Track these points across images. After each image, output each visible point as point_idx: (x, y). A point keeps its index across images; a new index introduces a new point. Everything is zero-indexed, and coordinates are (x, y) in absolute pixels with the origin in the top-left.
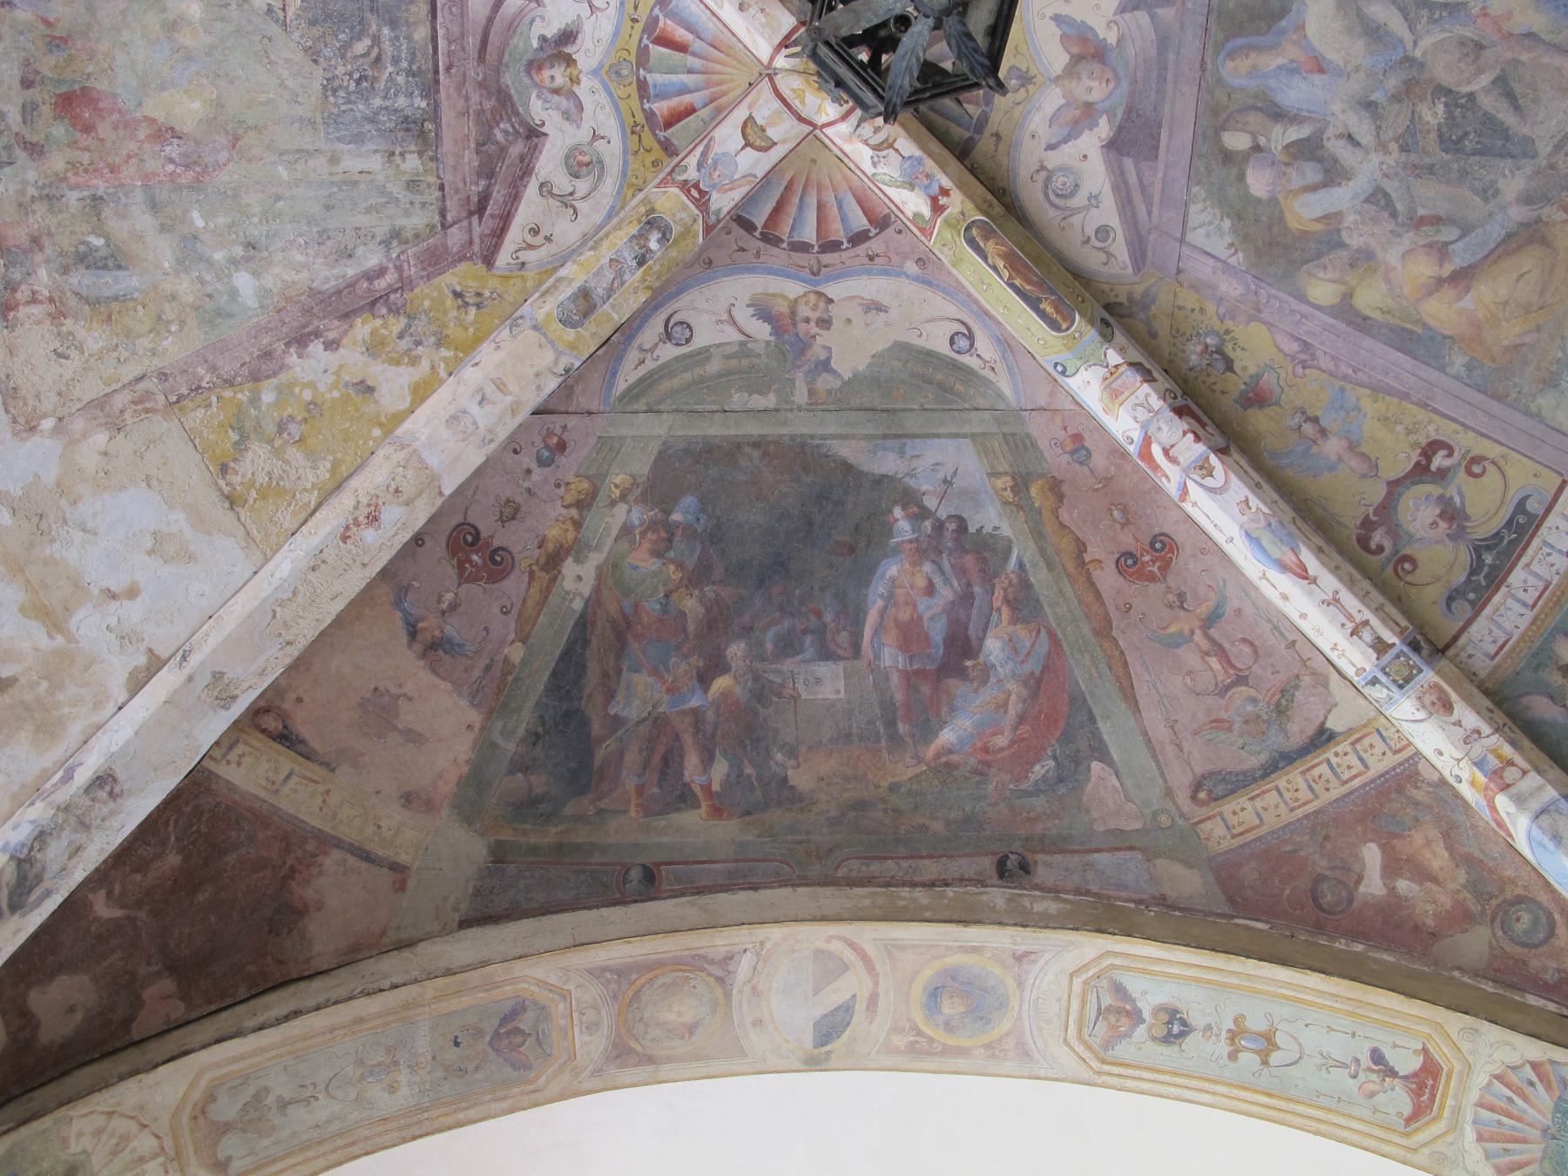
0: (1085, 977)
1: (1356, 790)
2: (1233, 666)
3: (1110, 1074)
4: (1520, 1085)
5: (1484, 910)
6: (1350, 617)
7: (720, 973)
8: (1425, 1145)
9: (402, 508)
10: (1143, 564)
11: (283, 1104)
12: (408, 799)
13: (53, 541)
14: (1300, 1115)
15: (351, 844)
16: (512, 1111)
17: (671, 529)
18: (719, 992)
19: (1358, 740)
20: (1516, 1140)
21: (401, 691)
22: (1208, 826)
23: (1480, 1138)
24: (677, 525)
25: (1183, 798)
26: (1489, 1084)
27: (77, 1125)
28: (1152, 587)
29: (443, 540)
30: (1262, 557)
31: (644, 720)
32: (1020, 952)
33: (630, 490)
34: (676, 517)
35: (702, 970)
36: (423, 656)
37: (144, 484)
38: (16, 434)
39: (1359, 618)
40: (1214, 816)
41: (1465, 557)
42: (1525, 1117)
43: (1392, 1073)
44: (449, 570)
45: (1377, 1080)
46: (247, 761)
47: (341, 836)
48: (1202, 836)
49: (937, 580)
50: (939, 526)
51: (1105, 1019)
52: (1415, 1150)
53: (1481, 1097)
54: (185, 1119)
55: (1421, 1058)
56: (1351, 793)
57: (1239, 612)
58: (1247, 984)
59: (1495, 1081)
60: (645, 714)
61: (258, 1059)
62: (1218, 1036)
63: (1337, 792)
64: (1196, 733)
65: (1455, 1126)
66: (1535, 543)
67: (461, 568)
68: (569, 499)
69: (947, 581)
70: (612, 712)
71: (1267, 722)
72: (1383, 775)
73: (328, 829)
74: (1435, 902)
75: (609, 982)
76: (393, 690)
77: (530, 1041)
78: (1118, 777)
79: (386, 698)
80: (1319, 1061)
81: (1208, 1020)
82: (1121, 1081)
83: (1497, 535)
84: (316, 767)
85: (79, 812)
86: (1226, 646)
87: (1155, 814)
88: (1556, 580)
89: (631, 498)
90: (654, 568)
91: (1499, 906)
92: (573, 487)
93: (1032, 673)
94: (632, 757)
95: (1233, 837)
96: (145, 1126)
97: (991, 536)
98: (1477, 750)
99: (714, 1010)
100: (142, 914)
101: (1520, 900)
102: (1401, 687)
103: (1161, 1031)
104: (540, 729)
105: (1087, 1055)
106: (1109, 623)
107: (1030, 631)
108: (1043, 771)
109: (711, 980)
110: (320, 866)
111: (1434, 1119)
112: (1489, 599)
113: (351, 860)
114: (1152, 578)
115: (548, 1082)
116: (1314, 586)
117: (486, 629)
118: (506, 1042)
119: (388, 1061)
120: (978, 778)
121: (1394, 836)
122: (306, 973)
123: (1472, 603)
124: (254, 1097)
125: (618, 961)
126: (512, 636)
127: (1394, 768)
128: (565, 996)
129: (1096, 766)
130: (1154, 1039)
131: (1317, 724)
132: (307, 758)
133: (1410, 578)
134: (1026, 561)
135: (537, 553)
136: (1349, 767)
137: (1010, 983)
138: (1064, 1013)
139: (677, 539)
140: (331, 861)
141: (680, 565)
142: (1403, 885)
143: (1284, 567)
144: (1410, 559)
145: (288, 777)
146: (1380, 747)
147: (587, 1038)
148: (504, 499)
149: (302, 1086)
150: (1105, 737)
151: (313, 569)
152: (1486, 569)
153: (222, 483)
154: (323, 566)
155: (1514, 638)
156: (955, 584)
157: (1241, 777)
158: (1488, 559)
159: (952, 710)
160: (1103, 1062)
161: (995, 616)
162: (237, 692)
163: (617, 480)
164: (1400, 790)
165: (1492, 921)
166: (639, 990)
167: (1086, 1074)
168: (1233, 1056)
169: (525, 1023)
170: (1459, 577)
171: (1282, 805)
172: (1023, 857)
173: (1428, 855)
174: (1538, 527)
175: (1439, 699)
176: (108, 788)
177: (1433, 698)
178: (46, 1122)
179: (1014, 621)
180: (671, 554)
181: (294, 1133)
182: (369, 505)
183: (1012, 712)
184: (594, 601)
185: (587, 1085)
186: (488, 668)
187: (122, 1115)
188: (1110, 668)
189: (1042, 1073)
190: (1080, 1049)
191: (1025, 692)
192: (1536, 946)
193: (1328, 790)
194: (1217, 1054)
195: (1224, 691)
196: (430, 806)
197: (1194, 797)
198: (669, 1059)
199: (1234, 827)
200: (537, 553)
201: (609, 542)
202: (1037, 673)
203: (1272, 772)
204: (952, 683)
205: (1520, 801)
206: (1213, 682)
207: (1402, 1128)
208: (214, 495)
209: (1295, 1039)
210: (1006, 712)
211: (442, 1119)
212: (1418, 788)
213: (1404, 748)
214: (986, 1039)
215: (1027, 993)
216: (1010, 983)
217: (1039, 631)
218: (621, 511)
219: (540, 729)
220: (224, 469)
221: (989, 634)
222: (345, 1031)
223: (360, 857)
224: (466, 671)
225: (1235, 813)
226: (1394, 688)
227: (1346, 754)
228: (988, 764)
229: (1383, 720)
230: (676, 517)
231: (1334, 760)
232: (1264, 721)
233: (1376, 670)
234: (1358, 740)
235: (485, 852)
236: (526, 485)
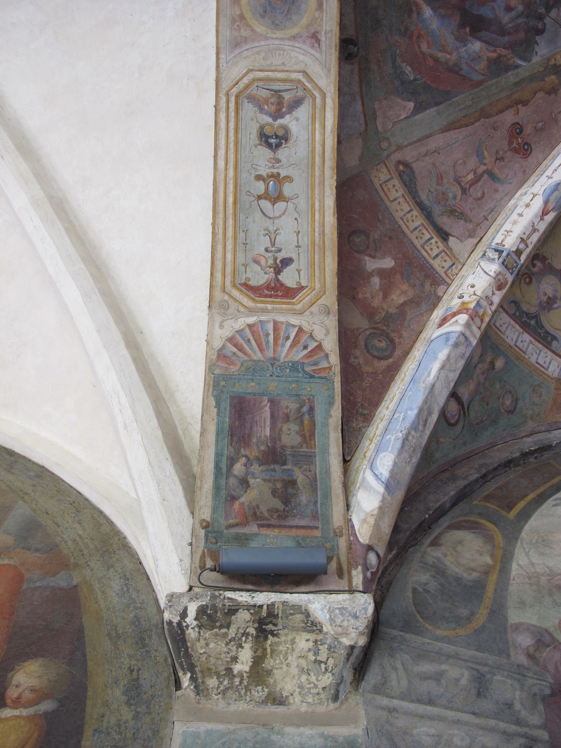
0: (304, 80)
1: (420, 253)
2: (471, 186)
3: (228, 102)
4: (302, 342)
5: (378, 323)
6: (529, 237)
8: (231, 296)
10: (517, 138)
14: (225, 222)
19: (446, 254)
20: (259, 346)
22: (384, 170)
23: (250, 326)
25: (397, 156)
26: (294, 326)
28: (506, 142)
30: (548, 192)
32: (318, 35)
39: (529, 242)
40: (390, 174)
41: (533, 310)
42: (279, 348)
43: (278, 271)
45: (269, 264)
48: (379, 167)
49: (513, 14)
50: (541, 18)
51: (272, 96)
52: (224, 290)
53: (282, 323)
55: (295, 286)
56: (418, 251)
57: (496, 191)
58: (317, 181)
59: (297, 328)
62: (273, 167)
63: (418, 243)
64: (434, 165)
65: (251, 311)
66: (540, 346)
69: (512, 20)
71: (445, 205)
72: (432, 267)
74: (373, 298)
78: (406, 118)
80: (271, 228)
81: (284, 160)
82: (224, 109)
83: (542, 327)
86: (480, 183)
87: (388, 139)
88: (527, 357)
91: (384, 330)
93: (461, 69)
95: (380, 185)
97: (533, 50)
98: (484, 303)
101: (392, 341)
102: (503, 263)
103: (268, 131)
105: (241, 85)
106: (488, 116)
107: (483, 70)
108: (407, 72)
111: (253, 300)
112: (517, 323)
114: (510, 143)
116: (539, 219)
120: (403, 30)
121: (402, 274)
123: (515, 314)
127: (437, 273)
129: (411, 105)
130: (262, 128)
131: (451, 233)
133: (523, 281)
134: (519, 70)
136: (431, 249)
137: (295, 31)
138: (273, 68)
142: (376, 281)
143: (546, 202)
144: (530, 282)
146: (447, 265)
150: (428, 111)
152: (528, 321)
155: (503, 336)
156: (510, 25)
157: (414, 190)
158: (533, 322)
159: (443, 17)
160: (237, 97)
161: (492, 49)
164: (427, 276)
165: (373, 328)
167: (225, 86)
168: (259, 178)
170: (525, 307)
171: (403, 213)
172: (356, 56)
173: (398, 292)
174: (546, 347)
175: (502, 283)
177: (502, 280)
179: (489, 60)
183: (440, 55)
188: (464, 116)
189: (222, 56)
190: (246, 80)
191: (451, 64)
192: (368, 351)
193: (417, 238)
194: (258, 167)
195: (458, 181)
197: (399, 162)
199: (386, 185)
202: (461, 72)
203: (420, 207)
204: (458, 18)
205: (467, 325)
206: (461, 175)
207: (237, 282)
209: (284, 213)
210: (440, 51)
212: (431, 285)
213: (449, 278)
214: (248, 15)
215: (287, 43)
216: (295, 31)
217: (484, 75)
221: (483, 44)
225: (394, 186)
226: (501, 260)
227: (438, 247)
228: (411, 37)
229: (460, 266)
231: (433, 241)
232: (445, 203)
233: (508, 250)
234: (446, 254)
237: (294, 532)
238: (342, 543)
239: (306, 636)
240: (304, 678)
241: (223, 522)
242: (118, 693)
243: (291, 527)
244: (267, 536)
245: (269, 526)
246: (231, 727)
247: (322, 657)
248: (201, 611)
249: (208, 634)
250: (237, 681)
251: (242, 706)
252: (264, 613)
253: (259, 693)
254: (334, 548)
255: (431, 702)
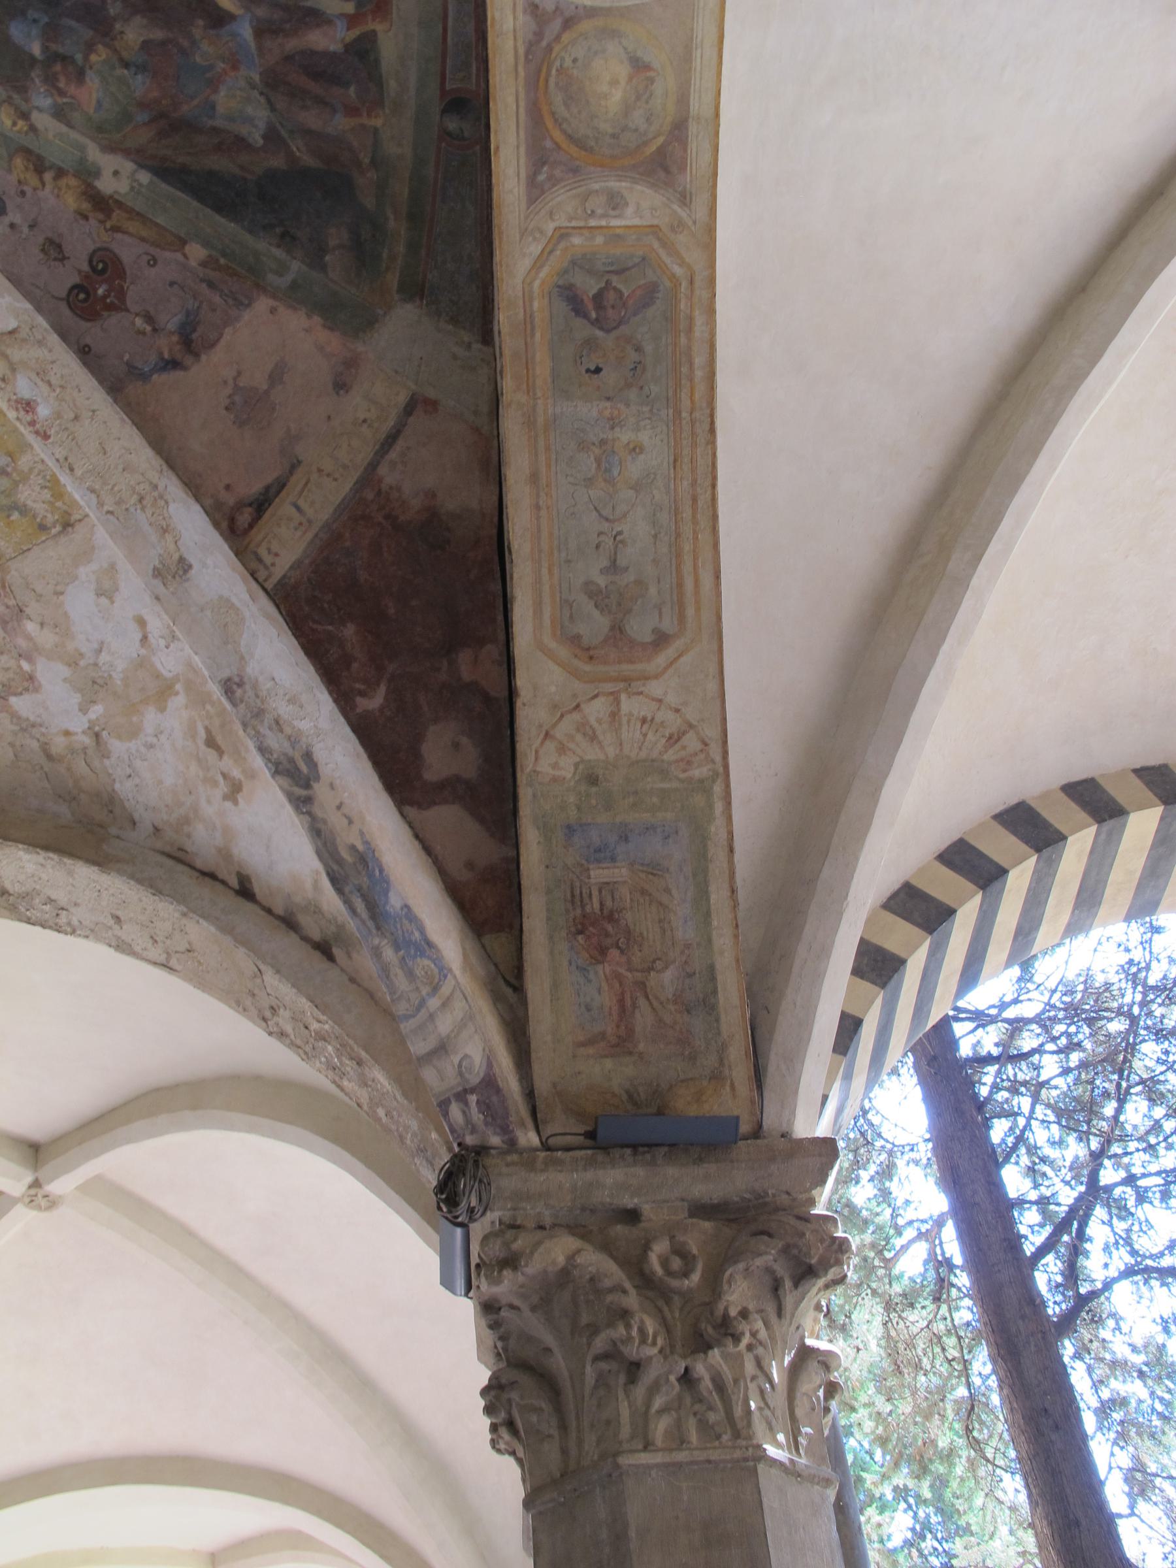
7: (557, 24)
9: (19, 376)
11: (613, 567)
12: (341, 386)
13: (110, 676)
15: (376, 453)
16: (711, 311)
17: (53, 58)
18: (585, 26)
21: (231, 382)
24: (45, 49)
27: (544, 767)
29: (85, 325)
31: (269, 101)
33: (17, 109)
34: (36, 49)
35: (549, 49)
36: (197, 355)
37: (61, 597)
38: (37, 690)
44: (114, 320)
46: (275, 547)
47: (366, 463)
54: (587, 668)
60: (262, 100)
61: (546, 588)
67: (111, 308)
68: (34, 181)
70: (261, 142)
73: (355, 475)
75: (550, 177)
76: (228, 390)
77: (616, 281)
79: (237, 398)
84: (293, 479)
85: (249, 715)
89: (24, 107)
90: (97, 81)
92: (22, 176)
94: (311, 119)
96: (578, 706)
99: (614, 34)
100: (391, 667)
104: (278, 230)
109: (566, 38)
110: (391, 488)
113: (393, 455)
115: (682, 263)
117: (172, 284)
118: (610, 312)
119: (597, 451)
122: (496, 519)
124: (590, 597)
125: (523, 160)
126: (179, 256)
128: (562, 234)
132: (283, 486)
135: (93, 222)
139: (61, 50)
140: (388, 475)
141: (90, 47)
145: (298, 509)
147: (630, 211)
148: (42, 256)
149: (597, 547)
151: (72, 469)
153: (54, 531)
154: (70, 460)
162: (176, 556)
163: (8, 123)
166: (570, 137)
169: (589, 286)
176: (235, 687)
178: (525, 794)
180: (79, 57)
181: (654, 560)
182: (17, 409)
184: (141, 158)
185: (701, 213)
186: (211, 285)
187: (554, 725)
196: (352, 363)
198: (683, 99)
200: (93, 222)
201: (74, 135)
208: (63, 539)
211: (697, 396)
218: (43, 120)
219: (278, 230)
220: (43, 528)
222: (542, 494)
223: (391, 446)
224: (214, 310)
230: (36, 49)
235: (409, 306)
236: (25, 230)
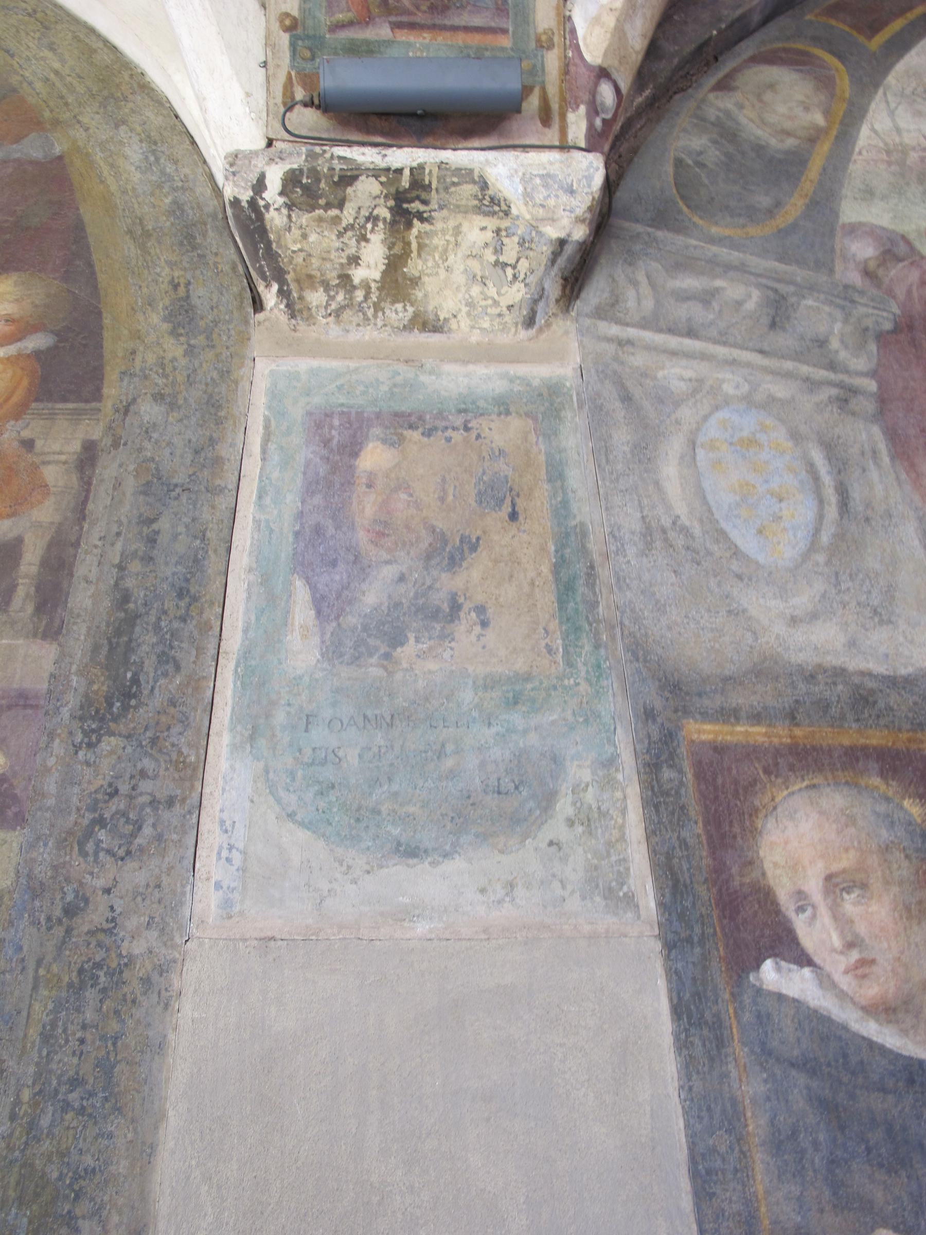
237: (460, 39)
238: (552, 61)
239: (480, 221)
240: (476, 290)
241: (324, 18)
242: (155, 319)
243: (455, 29)
244: (409, 45)
245: (412, 26)
246: (352, 364)
247: (509, 255)
248: (291, 181)
249: (304, 219)
250: (359, 295)
251: (369, 334)
252: (405, 182)
253: (398, 313)
254: (536, 71)
255: (691, 333)
